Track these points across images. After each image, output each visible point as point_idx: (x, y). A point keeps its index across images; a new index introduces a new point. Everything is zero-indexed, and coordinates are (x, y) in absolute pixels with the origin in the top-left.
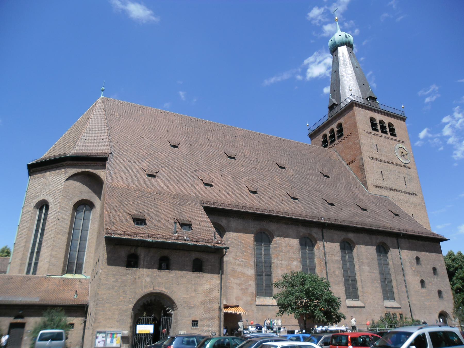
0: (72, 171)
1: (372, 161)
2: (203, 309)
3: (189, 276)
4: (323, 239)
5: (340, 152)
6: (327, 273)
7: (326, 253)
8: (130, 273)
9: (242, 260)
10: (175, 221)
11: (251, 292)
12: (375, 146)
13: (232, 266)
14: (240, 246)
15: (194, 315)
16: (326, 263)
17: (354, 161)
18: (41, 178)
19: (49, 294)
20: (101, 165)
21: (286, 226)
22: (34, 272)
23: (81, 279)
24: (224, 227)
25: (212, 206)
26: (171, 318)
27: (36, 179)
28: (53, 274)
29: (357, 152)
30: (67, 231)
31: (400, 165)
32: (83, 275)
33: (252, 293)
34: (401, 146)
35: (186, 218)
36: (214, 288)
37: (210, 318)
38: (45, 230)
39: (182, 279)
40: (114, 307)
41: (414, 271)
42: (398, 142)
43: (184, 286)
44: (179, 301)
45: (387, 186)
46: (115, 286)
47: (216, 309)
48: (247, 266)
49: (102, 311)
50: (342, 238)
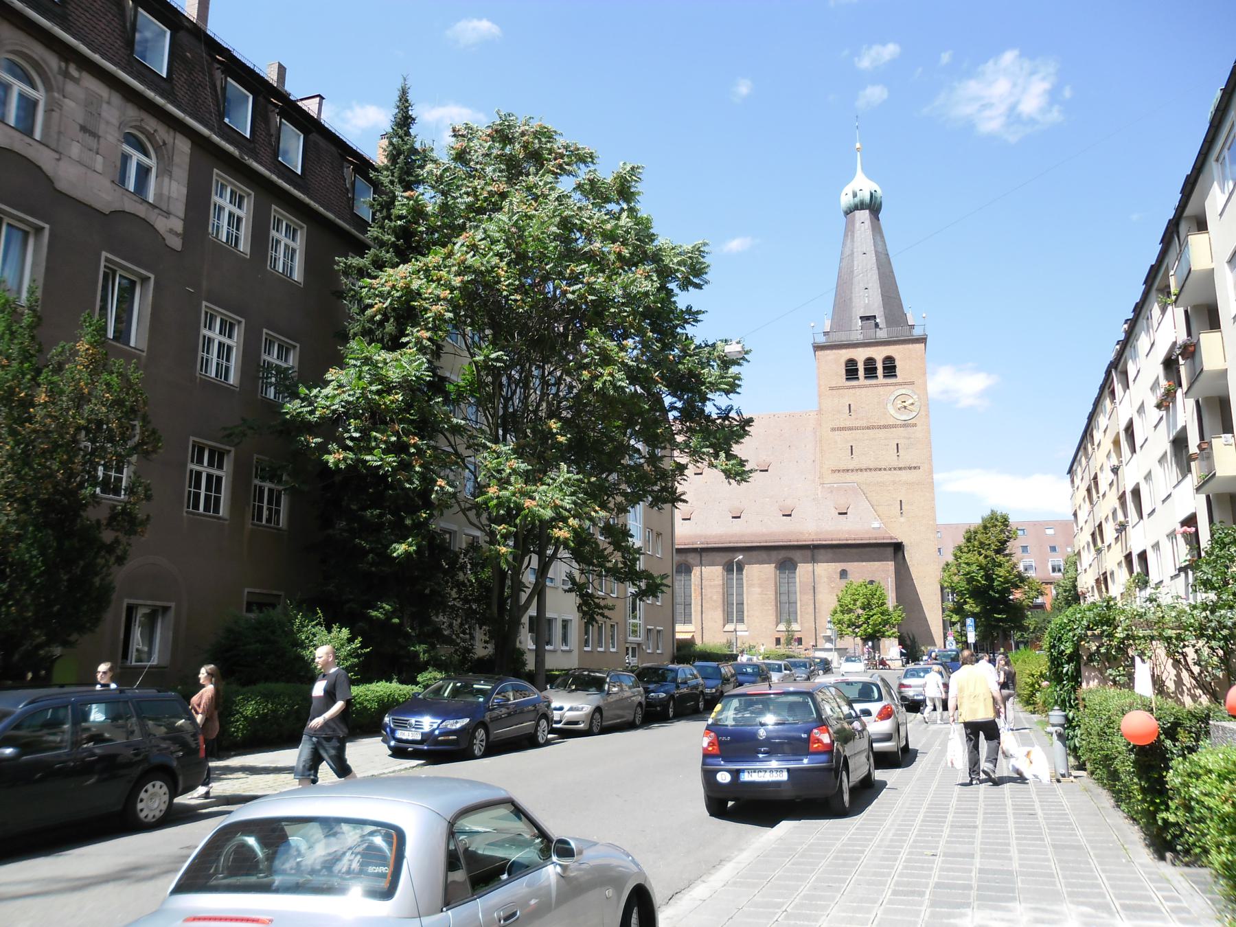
4: (701, 563)
12: (848, 408)
34: (903, 391)
41: (833, 588)
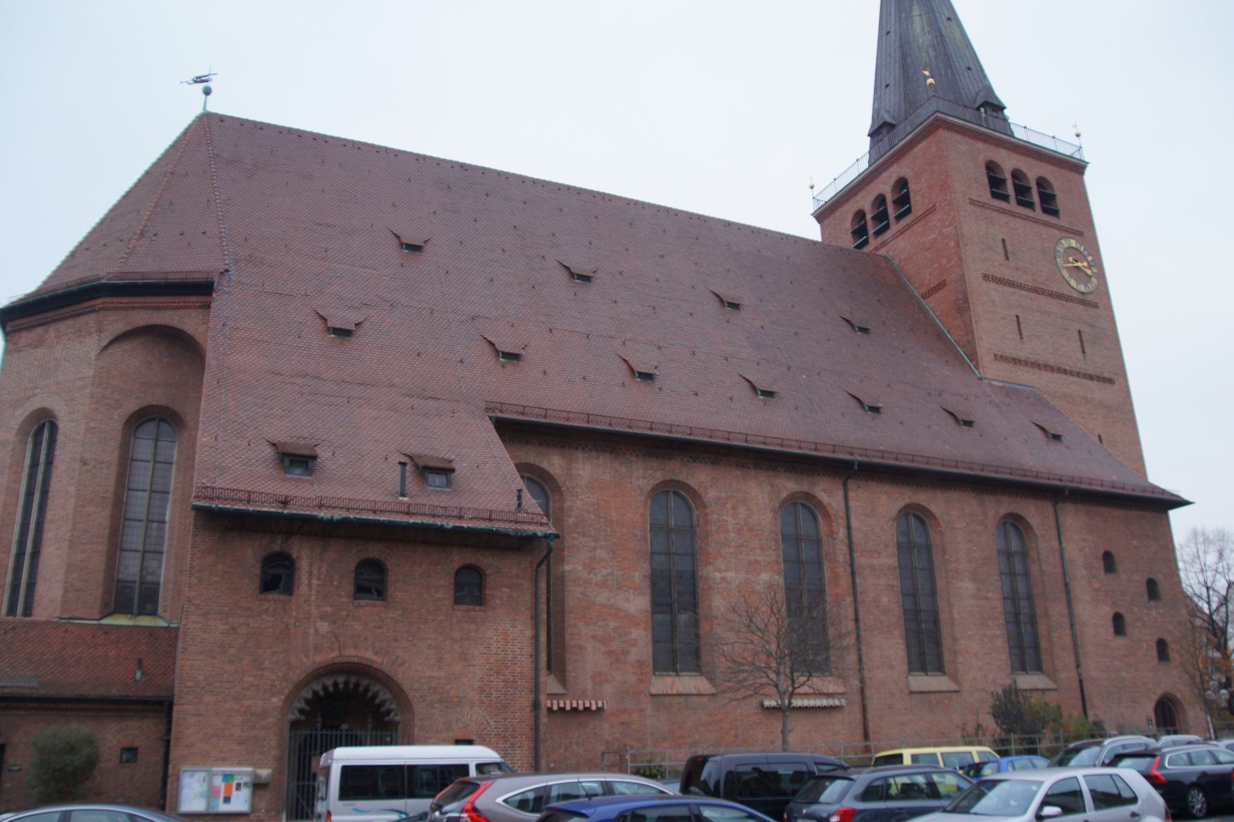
0: (117, 323)
1: (992, 285)
2: (485, 709)
3: (443, 618)
5: (902, 263)
6: (855, 600)
7: (855, 548)
8: (271, 609)
9: (610, 570)
10: (403, 461)
11: (637, 661)
12: (1001, 244)
13: (582, 589)
14: (605, 531)
15: (461, 725)
16: (853, 574)
17: (941, 286)
18: (33, 348)
19: (66, 669)
20: (199, 304)
21: (738, 473)
22: (28, 611)
23: (155, 628)
24: (556, 477)
25: (521, 418)
26: (397, 733)
27: (21, 351)
28: (77, 615)
29: (949, 261)
30: (110, 495)
31: (1069, 299)
32: (160, 617)
33: (640, 663)
34: (1073, 243)
35: (437, 448)
36: (519, 650)
37: (507, 734)
38: (50, 494)
39: (422, 626)
40: (228, 705)
41: (1096, 590)
42: (1063, 234)
43: (430, 645)
44: (416, 685)
45: (1033, 358)
46: (230, 647)
47: (524, 708)
48: (625, 588)
49: (195, 715)
50: (902, 504)
